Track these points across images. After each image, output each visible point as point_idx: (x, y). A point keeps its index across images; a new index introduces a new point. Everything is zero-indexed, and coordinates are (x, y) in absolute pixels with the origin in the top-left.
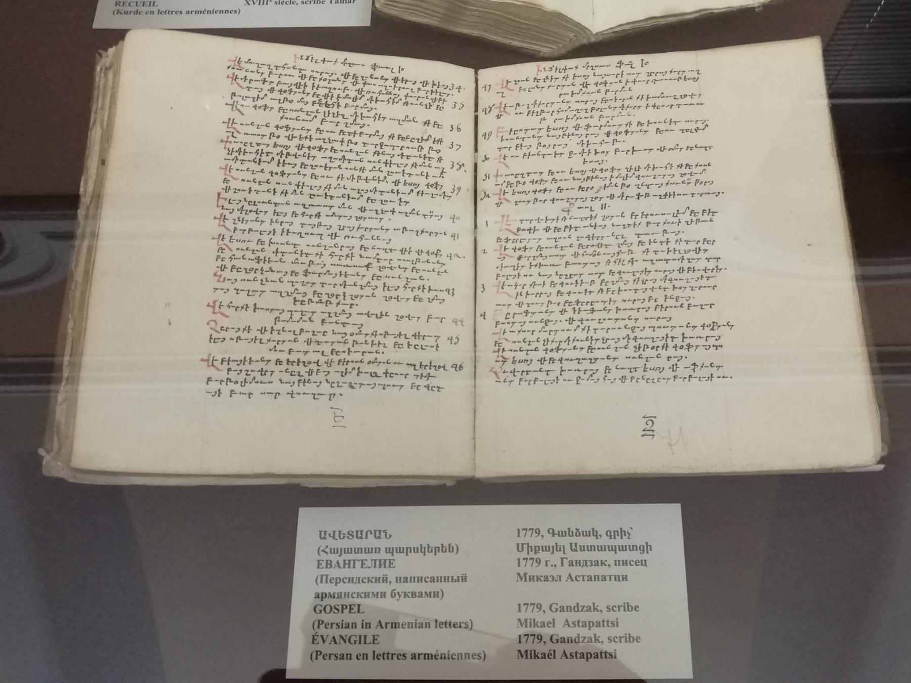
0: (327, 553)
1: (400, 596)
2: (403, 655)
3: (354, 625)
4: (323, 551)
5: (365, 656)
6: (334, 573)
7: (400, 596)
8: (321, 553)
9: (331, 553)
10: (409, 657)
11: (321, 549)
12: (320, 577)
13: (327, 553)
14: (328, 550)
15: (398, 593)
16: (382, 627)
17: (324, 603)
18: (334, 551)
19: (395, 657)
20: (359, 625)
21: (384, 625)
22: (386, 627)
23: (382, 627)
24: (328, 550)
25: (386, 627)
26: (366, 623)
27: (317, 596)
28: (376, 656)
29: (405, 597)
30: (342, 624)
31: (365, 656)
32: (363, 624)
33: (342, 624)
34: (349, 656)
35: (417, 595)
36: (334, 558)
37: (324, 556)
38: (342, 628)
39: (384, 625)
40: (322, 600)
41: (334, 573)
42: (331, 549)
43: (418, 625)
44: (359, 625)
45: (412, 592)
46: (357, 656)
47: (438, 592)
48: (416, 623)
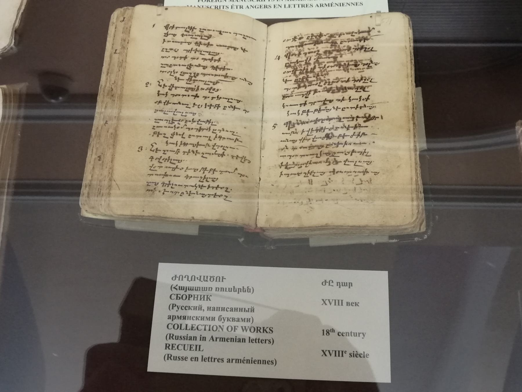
0: (177, 289)
1: (224, 320)
2: (222, 360)
3: (195, 338)
4: (174, 288)
5: (196, 359)
6: (180, 303)
7: (224, 320)
8: (173, 289)
9: (179, 289)
10: (225, 361)
11: (173, 287)
12: (171, 306)
13: (177, 289)
14: (177, 287)
15: (223, 318)
16: (213, 340)
17: (174, 323)
18: (181, 288)
19: (216, 360)
20: (198, 339)
21: (215, 339)
22: (216, 341)
23: (213, 340)
24: (177, 287)
25: (216, 341)
26: (203, 338)
27: (169, 317)
28: (203, 359)
29: (228, 321)
30: (187, 337)
31: (196, 359)
32: (201, 338)
33: (187, 337)
34: (185, 359)
35: (236, 320)
36: (182, 292)
37: (175, 292)
38: (187, 339)
39: (215, 339)
40: (173, 320)
41: (180, 303)
42: (179, 287)
43: (237, 340)
44: (198, 339)
45: (233, 318)
46: (191, 358)
47: (250, 319)
48: (236, 339)
